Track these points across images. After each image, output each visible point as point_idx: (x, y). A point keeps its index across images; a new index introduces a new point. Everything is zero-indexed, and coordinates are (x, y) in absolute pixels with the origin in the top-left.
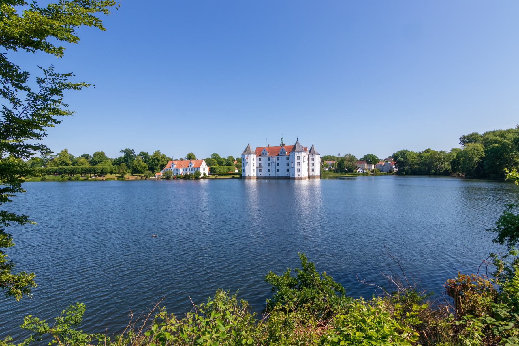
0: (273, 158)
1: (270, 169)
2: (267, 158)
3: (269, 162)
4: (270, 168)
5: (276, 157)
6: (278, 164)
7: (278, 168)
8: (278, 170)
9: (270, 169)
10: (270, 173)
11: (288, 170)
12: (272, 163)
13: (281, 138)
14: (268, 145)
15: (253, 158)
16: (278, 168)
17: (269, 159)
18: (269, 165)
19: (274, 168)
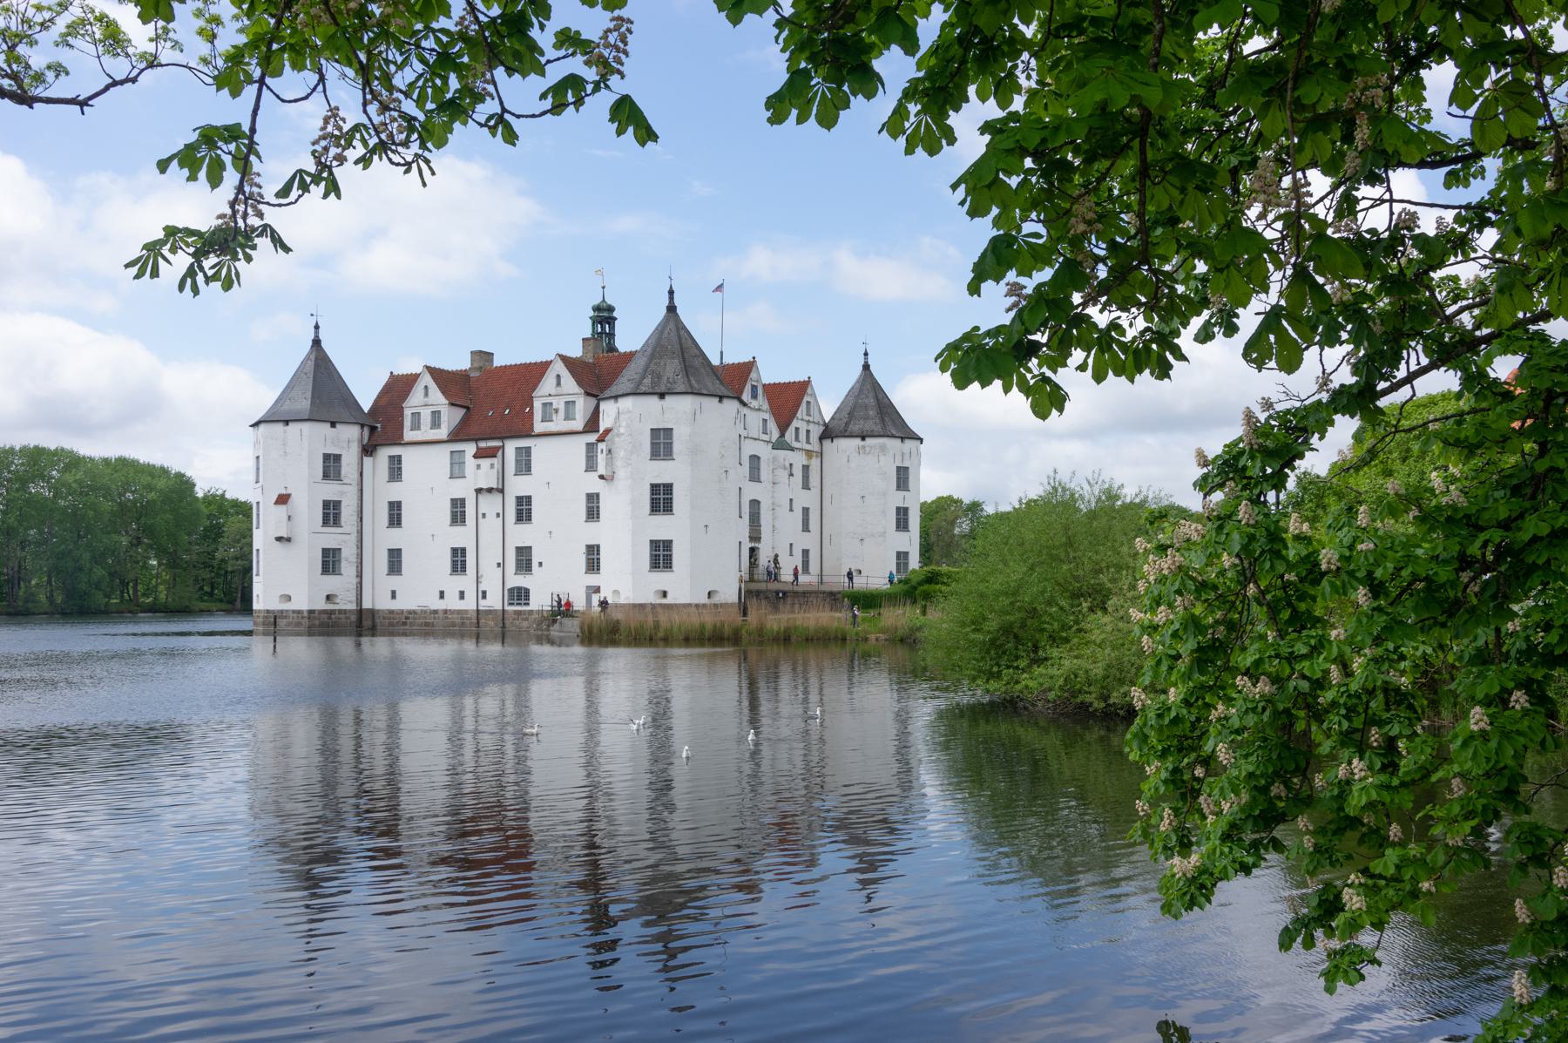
0: (485, 463)
1: (463, 550)
3: (463, 489)
4: (462, 536)
5: (511, 447)
6: (524, 510)
7: (521, 535)
8: (524, 560)
9: (463, 550)
10: (466, 582)
11: (593, 557)
12: (483, 498)
13: (597, 301)
16: (521, 535)
17: (457, 472)
18: (458, 513)
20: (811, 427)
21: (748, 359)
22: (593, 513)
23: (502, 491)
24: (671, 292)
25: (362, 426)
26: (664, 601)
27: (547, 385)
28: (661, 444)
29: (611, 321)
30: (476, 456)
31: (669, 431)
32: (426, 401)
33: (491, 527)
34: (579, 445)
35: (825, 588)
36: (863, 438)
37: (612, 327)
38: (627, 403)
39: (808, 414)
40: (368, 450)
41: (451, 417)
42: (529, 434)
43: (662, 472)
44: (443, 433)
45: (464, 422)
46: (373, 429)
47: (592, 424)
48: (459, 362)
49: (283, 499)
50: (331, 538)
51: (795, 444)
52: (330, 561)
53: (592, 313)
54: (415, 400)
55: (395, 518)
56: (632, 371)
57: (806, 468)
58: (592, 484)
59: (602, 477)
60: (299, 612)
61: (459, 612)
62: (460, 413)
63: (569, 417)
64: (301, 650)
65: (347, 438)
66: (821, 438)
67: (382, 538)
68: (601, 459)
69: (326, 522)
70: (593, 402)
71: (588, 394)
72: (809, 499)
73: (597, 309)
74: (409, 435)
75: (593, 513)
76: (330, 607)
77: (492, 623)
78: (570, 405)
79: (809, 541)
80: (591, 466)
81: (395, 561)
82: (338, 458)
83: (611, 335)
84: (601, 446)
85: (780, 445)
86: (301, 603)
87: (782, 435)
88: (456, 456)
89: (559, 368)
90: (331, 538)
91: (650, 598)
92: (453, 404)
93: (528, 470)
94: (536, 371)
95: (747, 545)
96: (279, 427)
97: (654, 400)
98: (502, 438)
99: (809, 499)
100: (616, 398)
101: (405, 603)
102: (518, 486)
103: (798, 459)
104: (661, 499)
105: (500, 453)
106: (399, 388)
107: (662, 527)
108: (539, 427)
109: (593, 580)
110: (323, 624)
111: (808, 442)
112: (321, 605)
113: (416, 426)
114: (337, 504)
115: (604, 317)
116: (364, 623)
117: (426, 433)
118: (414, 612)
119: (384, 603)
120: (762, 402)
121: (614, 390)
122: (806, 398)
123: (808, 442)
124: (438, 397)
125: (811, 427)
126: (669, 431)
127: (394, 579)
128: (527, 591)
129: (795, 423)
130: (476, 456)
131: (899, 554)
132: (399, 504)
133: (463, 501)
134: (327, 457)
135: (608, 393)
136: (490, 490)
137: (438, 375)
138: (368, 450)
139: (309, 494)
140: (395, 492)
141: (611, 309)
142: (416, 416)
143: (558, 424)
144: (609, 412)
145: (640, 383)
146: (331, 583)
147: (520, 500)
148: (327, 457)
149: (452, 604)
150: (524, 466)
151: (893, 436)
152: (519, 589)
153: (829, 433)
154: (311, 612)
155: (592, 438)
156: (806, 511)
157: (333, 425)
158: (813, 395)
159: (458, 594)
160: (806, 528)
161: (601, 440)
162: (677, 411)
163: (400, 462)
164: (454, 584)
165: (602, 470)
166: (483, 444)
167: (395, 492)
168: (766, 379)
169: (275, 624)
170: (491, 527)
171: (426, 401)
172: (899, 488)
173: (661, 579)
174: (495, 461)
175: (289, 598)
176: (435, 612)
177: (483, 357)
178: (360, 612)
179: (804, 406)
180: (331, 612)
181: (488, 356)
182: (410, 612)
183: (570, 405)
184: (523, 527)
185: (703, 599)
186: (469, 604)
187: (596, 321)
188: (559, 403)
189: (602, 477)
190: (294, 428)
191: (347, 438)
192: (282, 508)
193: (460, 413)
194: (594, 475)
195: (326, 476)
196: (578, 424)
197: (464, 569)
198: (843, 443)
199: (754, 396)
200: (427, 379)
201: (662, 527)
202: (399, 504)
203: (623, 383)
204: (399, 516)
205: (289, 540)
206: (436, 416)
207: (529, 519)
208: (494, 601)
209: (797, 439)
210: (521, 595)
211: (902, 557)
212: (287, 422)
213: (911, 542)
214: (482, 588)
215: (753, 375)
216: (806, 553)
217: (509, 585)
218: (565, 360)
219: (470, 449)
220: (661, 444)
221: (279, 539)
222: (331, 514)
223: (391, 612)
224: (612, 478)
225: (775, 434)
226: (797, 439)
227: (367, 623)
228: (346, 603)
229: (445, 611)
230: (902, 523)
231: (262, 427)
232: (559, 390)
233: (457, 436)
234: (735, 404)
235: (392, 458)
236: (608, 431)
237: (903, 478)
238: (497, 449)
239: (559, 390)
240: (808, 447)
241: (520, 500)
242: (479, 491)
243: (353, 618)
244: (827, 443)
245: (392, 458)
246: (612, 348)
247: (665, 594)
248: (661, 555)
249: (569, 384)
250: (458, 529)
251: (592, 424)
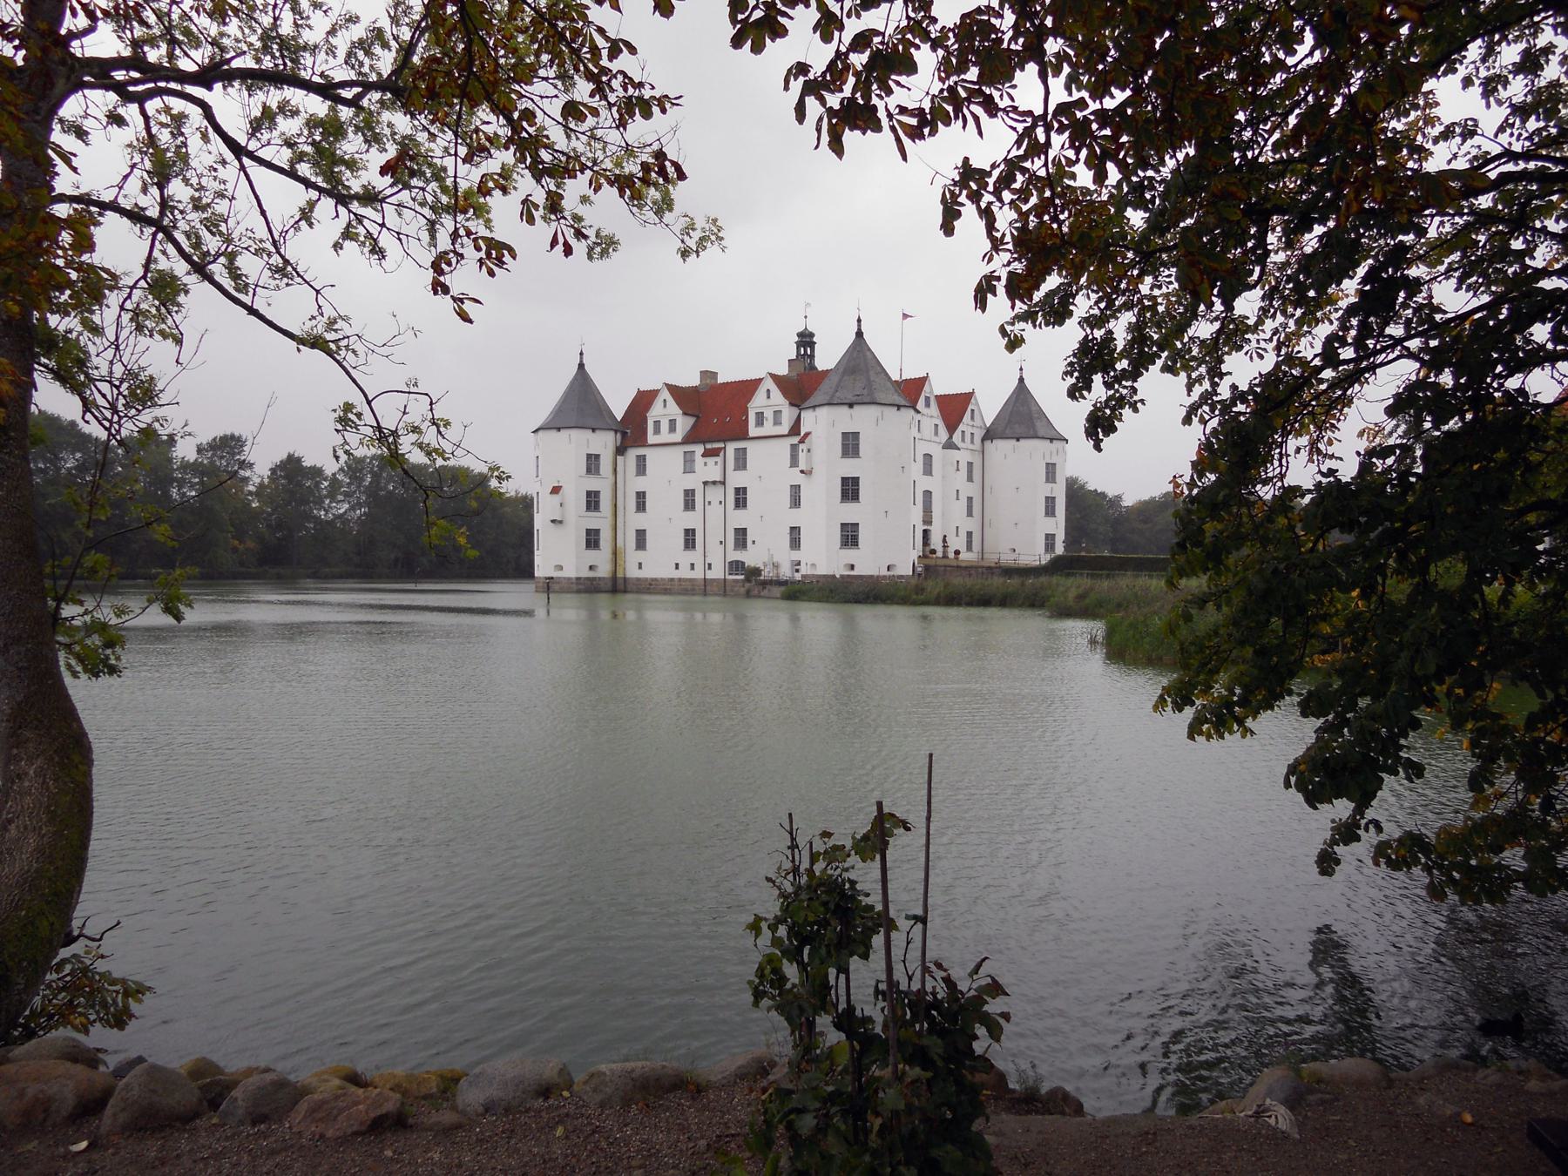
0: (711, 461)
1: (694, 530)
2: (677, 454)
3: (694, 482)
4: (692, 520)
5: (731, 448)
7: (738, 519)
8: (741, 537)
9: (694, 530)
10: (695, 556)
12: (710, 490)
14: (704, 374)
15: (593, 463)
16: (738, 519)
17: (689, 466)
19: (716, 519)
20: (975, 431)
21: (923, 375)
22: (796, 502)
23: (723, 483)
24: (859, 321)
25: (616, 431)
26: (852, 573)
27: (758, 402)
28: (850, 446)
29: (812, 345)
30: (704, 455)
31: (856, 435)
32: (664, 411)
33: (715, 512)
34: (784, 446)
35: (986, 564)
36: (1018, 440)
37: (813, 350)
38: (823, 412)
39: (972, 418)
40: (620, 451)
41: (684, 424)
42: (744, 436)
43: (850, 468)
44: (678, 436)
45: (694, 427)
46: (624, 434)
47: (795, 429)
48: (691, 380)
49: (556, 490)
50: (594, 521)
51: (960, 445)
52: (592, 539)
53: (797, 339)
54: (656, 412)
55: (641, 505)
56: (826, 387)
57: (970, 465)
58: (799, 479)
59: (802, 472)
60: (569, 579)
61: (691, 580)
62: (691, 421)
63: (777, 422)
64: (570, 611)
65: (604, 443)
66: (983, 440)
67: (633, 521)
68: (802, 456)
69: (588, 508)
70: (795, 411)
71: (792, 404)
72: (972, 490)
73: (800, 335)
74: (652, 439)
75: (796, 502)
76: (591, 574)
77: (715, 589)
78: (777, 413)
79: (972, 525)
80: (794, 462)
81: (641, 539)
82: (597, 457)
83: (812, 356)
84: (801, 446)
85: (949, 445)
86: (570, 572)
87: (951, 437)
88: (688, 455)
89: (769, 384)
90: (594, 521)
91: (839, 571)
92: (685, 414)
93: (744, 467)
94: (749, 387)
95: (920, 528)
96: (553, 433)
97: (845, 409)
98: (724, 441)
99: (972, 490)
100: (814, 407)
101: (646, 573)
102: (736, 479)
103: (963, 456)
104: (850, 490)
105: (722, 454)
106: (644, 400)
107: (850, 512)
108: (753, 431)
109: (795, 555)
110: (587, 587)
111: (972, 442)
112: (586, 574)
113: (657, 431)
114: (597, 494)
115: (806, 340)
116: (617, 586)
117: (665, 436)
118: (656, 580)
119: (633, 572)
120: (934, 410)
121: (812, 401)
122: (970, 407)
123: (972, 442)
124: (674, 409)
125: (975, 431)
126: (856, 435)
127: (640, 553)
128: (743, 563)
129: (961, 427)
130: (704, 455)
131: (1047, 535)
132: (644, 493)
133: (693, 491)
134: (589, 456)
135: (806, 404)
136: (714, 483)
137: (675, 391)
138: (620, 451)
139: (576, 487)
140: (640, 484)
141: (812, 335)
142: (657, 423)
143: (769, 428)
144: (809, 420)
145: (833, 396)
146: (593, 556)
147: (737, 490)
148: (589, 456)
149: (684, 573)
150: (741, 463)
151: (1043, 438)
152: (737, 562)
153: (990, 435)
154: (578, 579)
155: (795, 440)
156: (970, 499)
157: (594, 430)
158: (977, 404)
159: (689, 566)
160: (970, 514)
161: (802, 441)
162: (862, 419)
163: (645, 460)
164: (687, 558)
165: (802, 466)
166: (709, 446)
167: (640, 484)
168: (939, 391)
169: (549, 586)
170: (715, 512)
171: (664, 411)
172: (1048, 481)
173: (850, 555)
174: (719, 459)
175: (560, 568)
176: (672, 580)
177: (708, 375)
178: (614, 578)
179: (968, 413)
180: (594, 579)
181: (714, 375)
182: (653, 580)
183: (777, 413)
184: (738, 512)
185: (884, 572)
186: (698, 574)
187: (799, 345)
188: (769, 414)
189: (802, 472)
190: (564, 433)
191: (604, 443)
192: (556, 498)
193: (691, 421)
194: (796, 470)
195: (589, 471)
196: (785, 429)
197: (694, 547)
198: (999, 443)
199: (928, 405)
200: (666, 394)
201: (850, 512)
202: (644, 493)
203: (818, 397)
204: (644, 503)
205: (561, 522)
206: (673, 423)
207: (745, 506)
208: (717, 573)
209: (963, 440)
210: (736, 566)
211: (1050, 539)
212: (559, 429)
213: (1058, 526)
214: (708, 561)
215: (926, 388)
216: (970, 534)
217: (728, 560)
218: (774, 377)
219: (699, 449)
220: (850, 446)
221: (553, 521)
222: (593, 501)
223: (638, 579)
224: (810, 472)
225: (943, 434)
226: (963, 440)
227: (620, 585)
228: (604, 571)
229: (680, 579)
230: (1050, 511)
231: (540, 433)
232: (770, 401)
233: (689, 439)
234: (912, 412)
235: (638, 457)
236: (807, 434)
237: (1051, 472)
238: (720, 449)
239: (770, 401)
240: (971, 447)
241: (737, 490)
242: (705, 483)
243: (609, 585)
244: (988, 443)
245: (638, 457)
246: (813, 368)
247: (852, 567)
248: (850, 535)
249: (778, 397)
250: (690, 513)
251: (795, 429)
